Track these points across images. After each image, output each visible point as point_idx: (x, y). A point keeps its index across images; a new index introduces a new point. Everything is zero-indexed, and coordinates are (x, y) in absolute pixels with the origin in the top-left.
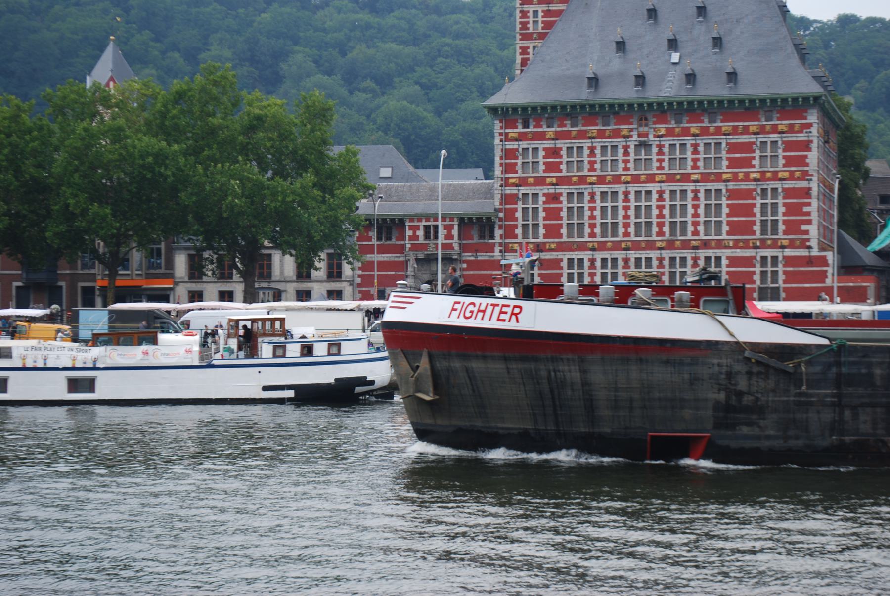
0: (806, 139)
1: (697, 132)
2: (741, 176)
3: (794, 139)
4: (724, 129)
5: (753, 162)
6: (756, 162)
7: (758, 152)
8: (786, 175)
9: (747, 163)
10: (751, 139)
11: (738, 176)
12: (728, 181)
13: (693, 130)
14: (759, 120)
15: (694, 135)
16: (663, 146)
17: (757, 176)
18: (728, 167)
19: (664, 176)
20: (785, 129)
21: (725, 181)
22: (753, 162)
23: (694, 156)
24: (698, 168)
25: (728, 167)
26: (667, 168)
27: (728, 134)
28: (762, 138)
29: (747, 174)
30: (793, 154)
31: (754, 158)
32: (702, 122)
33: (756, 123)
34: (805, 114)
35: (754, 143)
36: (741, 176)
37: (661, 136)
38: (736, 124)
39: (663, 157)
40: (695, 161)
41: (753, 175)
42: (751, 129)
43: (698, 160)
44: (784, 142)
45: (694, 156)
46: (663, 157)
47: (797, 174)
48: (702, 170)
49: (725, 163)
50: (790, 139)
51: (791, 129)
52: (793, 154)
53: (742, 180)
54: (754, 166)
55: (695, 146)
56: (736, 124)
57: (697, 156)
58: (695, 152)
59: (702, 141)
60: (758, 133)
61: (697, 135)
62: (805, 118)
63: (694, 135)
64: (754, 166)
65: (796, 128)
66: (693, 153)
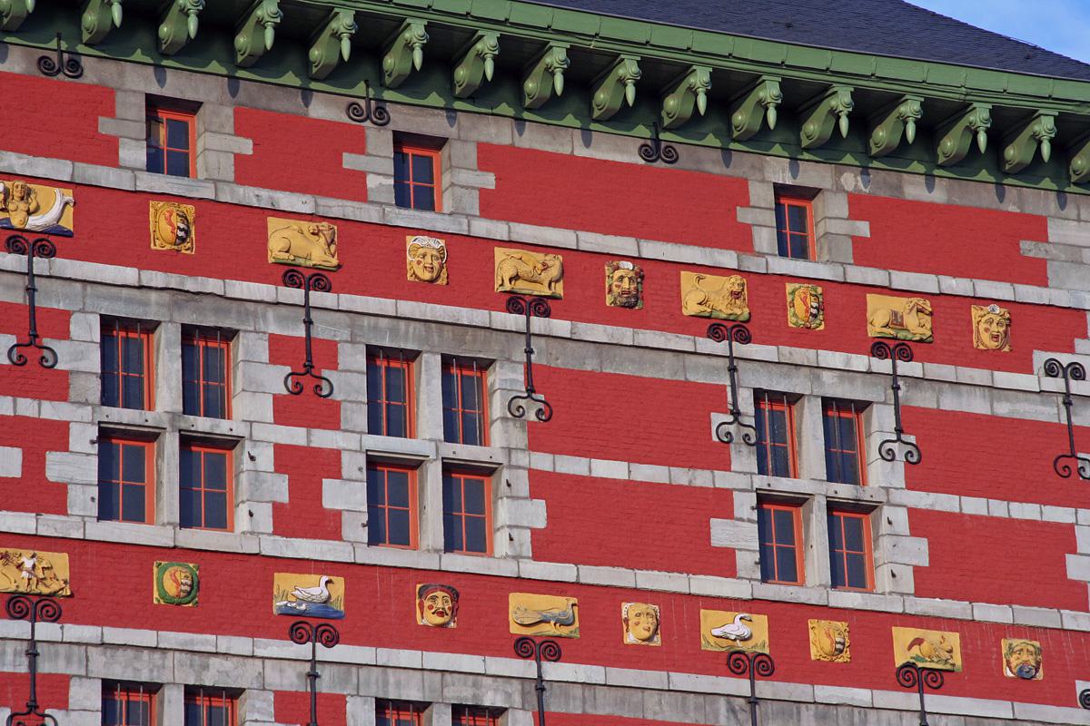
0: (1050, 413)
1: (318, 253)
2: (638, 625)
3: (977, 405)
4: (506, 264)
5: (720, 533)
6: (737, 533)
7: (744, 460)
8: (945, 648)
9: (676, 530)
10: (703, 360)
11: (619, 625)
12: (551, 650)
13: (282, 240)
14: (741, 240)
15: (291, 274)
16: (61, 324)
17: (754, 633)
18: (543, 547)
19: (60, 563)
20: (917, 326)
21: (523, 648)
22: (720, 533)
23: (295, 436)
24: (329, 526)
25: (543, 547)
26: (84, 499)
27: (541, 306)
28: (764, 363)
29: (680, 614)
30: (974, 506)
31: (721, 503)
32: (354, 187)
33: (728, 259)
34: (1028, 248)
35: (713, 397)
36: (638, 625)
37: (44, 243)
38: (591, 241)
39: (51, 411)
40: (306, 468)
41: (721, 629)
42: (695, 295)
43: (330, 463)
44: (906, 420)
45: (295, 436)
46: (51, 411)
47: (1017, 656)
48: (353, 546)
49: (516, 516)
50: (950, 402)
51: (949, 333)
52: (974, 506)
53: (640, 657)
54: (723, 563)
55: (306, 362)
56: (591, 241)
57: (324, 439)
58: (306, 399)
59: (354, 319)
60: (741, 331)
61: (318, 279)
62: (1036, 273)
63: (291, 274)
64: (723, 563)
65: (986, 328)
66: (284, 412)
